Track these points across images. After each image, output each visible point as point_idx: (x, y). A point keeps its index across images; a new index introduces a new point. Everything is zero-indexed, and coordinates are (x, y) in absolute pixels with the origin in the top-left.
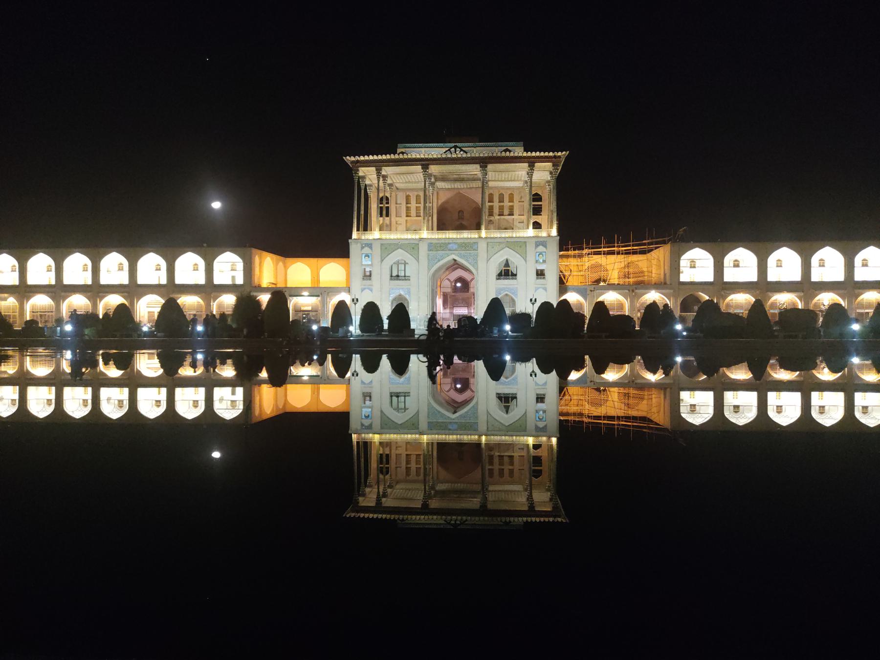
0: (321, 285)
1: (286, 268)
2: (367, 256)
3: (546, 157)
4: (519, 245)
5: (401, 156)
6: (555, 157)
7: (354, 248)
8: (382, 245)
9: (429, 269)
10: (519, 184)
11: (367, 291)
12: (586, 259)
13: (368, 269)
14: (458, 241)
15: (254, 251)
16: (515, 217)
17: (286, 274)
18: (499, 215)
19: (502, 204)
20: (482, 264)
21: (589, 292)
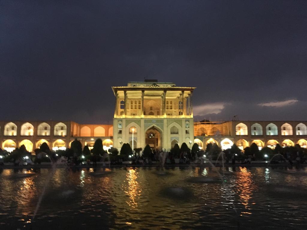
0: (94, 136)
1: (80, 128)
2: (120, 124)
3: (188, 89)
4: (179, 121)
5: (134, 87)
6: (192, 89)
7: (115, 122)
8: (126, 120)
9: (145, 130)
10: (175, 98)
11: (120, 139)
12: (197, 126)
13: (119, 130)
14: (156, 119)
15: (72, 122)
16: (173, 110)
17: (80, 131)
18: (167, 109)
19: (167, 105)
20: (165, 128)
21: (203, 139)
